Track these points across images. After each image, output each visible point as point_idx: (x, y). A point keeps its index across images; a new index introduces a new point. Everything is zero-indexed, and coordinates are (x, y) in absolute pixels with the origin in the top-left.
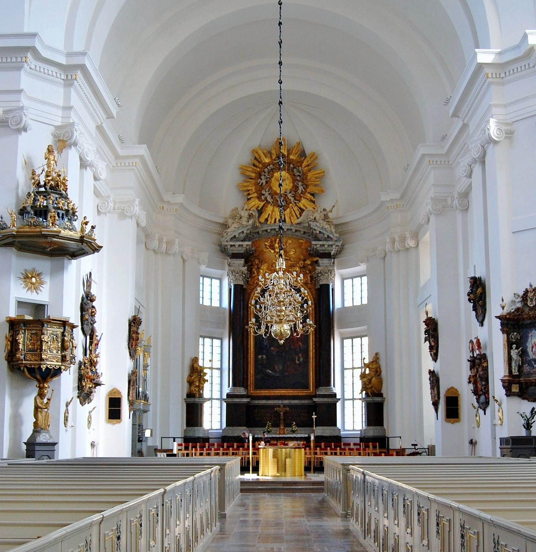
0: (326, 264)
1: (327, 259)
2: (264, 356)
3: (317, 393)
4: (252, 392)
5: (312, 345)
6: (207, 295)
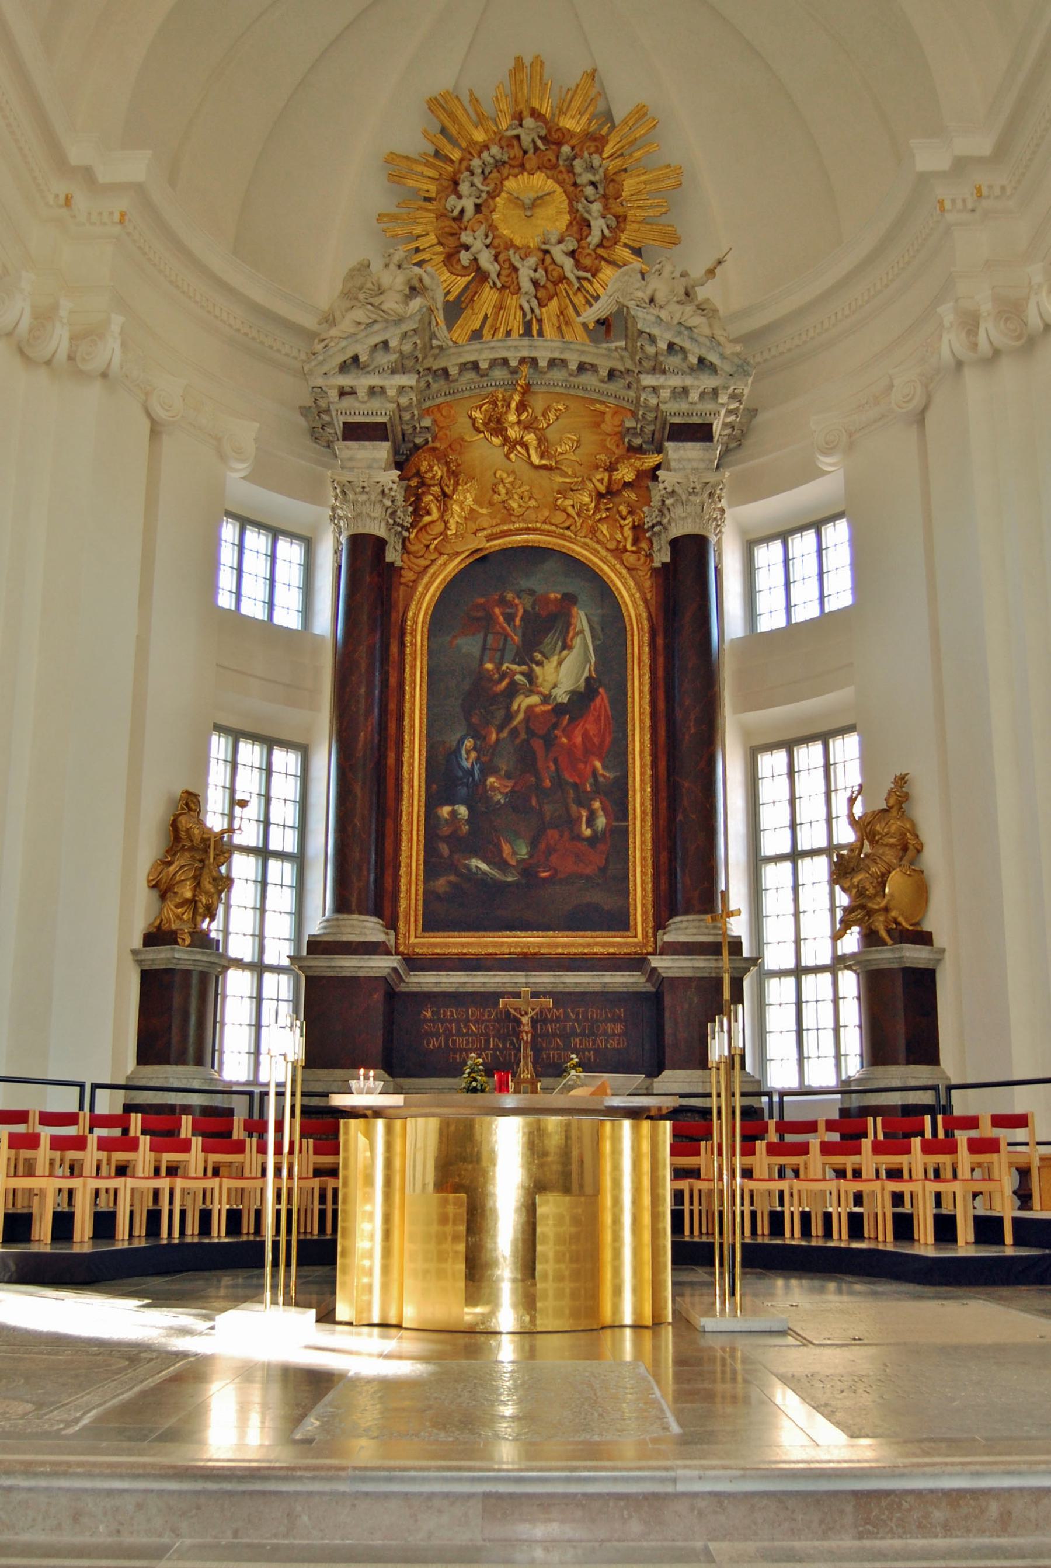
0: (695, 465)
1: (699, 445)
2: (463, 811)
3: (667, 938)
4: (413, 940)
5: (642, 766)
6: (254, 589)
